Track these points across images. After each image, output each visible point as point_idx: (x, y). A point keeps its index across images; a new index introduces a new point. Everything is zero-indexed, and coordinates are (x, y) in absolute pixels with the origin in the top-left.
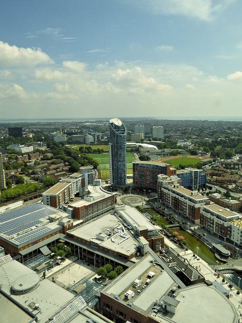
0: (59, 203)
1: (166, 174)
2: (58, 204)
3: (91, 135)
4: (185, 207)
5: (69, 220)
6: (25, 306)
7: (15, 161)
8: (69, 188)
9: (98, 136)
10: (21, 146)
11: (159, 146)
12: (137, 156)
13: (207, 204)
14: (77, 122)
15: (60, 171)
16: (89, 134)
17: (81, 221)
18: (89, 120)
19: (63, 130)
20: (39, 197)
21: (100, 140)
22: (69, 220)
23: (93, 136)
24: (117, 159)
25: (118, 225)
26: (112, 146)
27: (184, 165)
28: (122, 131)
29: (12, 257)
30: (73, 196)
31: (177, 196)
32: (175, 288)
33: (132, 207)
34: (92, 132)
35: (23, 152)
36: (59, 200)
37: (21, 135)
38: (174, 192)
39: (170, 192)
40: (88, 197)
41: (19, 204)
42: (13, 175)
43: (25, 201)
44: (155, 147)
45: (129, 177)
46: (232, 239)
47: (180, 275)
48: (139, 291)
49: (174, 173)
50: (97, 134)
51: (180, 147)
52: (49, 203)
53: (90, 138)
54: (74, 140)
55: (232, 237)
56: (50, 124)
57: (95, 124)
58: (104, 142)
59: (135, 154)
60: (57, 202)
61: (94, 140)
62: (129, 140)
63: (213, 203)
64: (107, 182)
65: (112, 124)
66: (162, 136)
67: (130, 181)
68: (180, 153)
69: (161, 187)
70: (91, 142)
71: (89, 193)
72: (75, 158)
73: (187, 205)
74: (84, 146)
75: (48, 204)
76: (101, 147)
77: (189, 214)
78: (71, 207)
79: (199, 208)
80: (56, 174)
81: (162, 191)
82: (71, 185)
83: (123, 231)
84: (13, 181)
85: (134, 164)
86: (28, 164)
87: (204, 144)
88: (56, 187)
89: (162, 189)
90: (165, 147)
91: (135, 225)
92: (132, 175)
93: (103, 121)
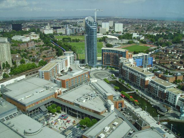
1: (125, 57)
9: (75, 29)
17: (66, 89)
23: (72, 29)
27: (137, 51)
30: (59, 72)
32: (131, 132)
33: (101, 80)
41: (24, 77)
42: (18, 58)
43: (27, 75)
44: (117, 38)
46: (168, 101)
49: (130, 56)
50: (75, 28)
55: (168, 100)
56: (41, 21)
62: (98, 33)
63: (157, 77)
76: (77, 38)
85: (103, 50)
88: (48, 66)
92: (101, 58)
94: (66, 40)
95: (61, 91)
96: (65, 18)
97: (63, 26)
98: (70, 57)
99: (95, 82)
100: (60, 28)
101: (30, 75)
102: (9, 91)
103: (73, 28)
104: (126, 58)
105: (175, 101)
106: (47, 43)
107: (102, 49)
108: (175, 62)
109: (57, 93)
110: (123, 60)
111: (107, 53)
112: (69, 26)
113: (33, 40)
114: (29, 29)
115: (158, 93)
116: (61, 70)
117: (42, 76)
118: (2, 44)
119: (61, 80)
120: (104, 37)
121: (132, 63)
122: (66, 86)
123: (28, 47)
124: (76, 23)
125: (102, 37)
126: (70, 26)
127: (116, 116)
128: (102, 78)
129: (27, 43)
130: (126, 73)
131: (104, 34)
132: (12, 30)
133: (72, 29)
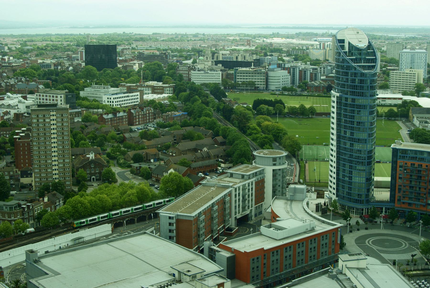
3: (284, 69)
5: (221, 281)
8: (222, 202)
12: (404, 132)
15: (203, 159)
16: (279, 66)
18: (282, 32)
20: (150, 218)
21: (306, 84)
22: (221, 281)
23: (291, 71)
24: (352, 134)
28: (368, 61)
30: (232, 223)
33: (384, 261)
37: (113, 64)
40: (270, 226)
42: (92, 161)
45: (380, 186)
50: (300, 65)
52: (174, 234)
54: (240, 80)
57: (295, 41)
58: (317, 88)
59: (400, 123)
61: (293, 82)
62: (385, 87)
65: (342, 41)
70: (285, 89)
71: (274, 217)
75: (171, 238)
80: (194, 165)
82: (230, 194)
84: (91, 174)
85: (395, 151)
86: (127, 135)
88: (193, 198)
92: (389, 179)
93: (316, 35)
94: (264, 107)
96: (269, 32)
97: (258, 57)
98: (274, 170)
99: (358, 269)
100: (247, 64)
101: (127, 223)
102: (50, 274)
103: (294, 68)
107: (393, 146)
111: (413, 165)
112: (279, 59)
113: (152, 103)
114: (140, 65)
116: (239, 216)
117: (170, 231)
118: (45, 113)
119: (236, 252)
120: (405, 103)
124: (308, 49)
125: (400, 102)
126: (283, 61)
128: (386, 256)
131: (404, 94)
132: (83, 64)
133: (291, 71)
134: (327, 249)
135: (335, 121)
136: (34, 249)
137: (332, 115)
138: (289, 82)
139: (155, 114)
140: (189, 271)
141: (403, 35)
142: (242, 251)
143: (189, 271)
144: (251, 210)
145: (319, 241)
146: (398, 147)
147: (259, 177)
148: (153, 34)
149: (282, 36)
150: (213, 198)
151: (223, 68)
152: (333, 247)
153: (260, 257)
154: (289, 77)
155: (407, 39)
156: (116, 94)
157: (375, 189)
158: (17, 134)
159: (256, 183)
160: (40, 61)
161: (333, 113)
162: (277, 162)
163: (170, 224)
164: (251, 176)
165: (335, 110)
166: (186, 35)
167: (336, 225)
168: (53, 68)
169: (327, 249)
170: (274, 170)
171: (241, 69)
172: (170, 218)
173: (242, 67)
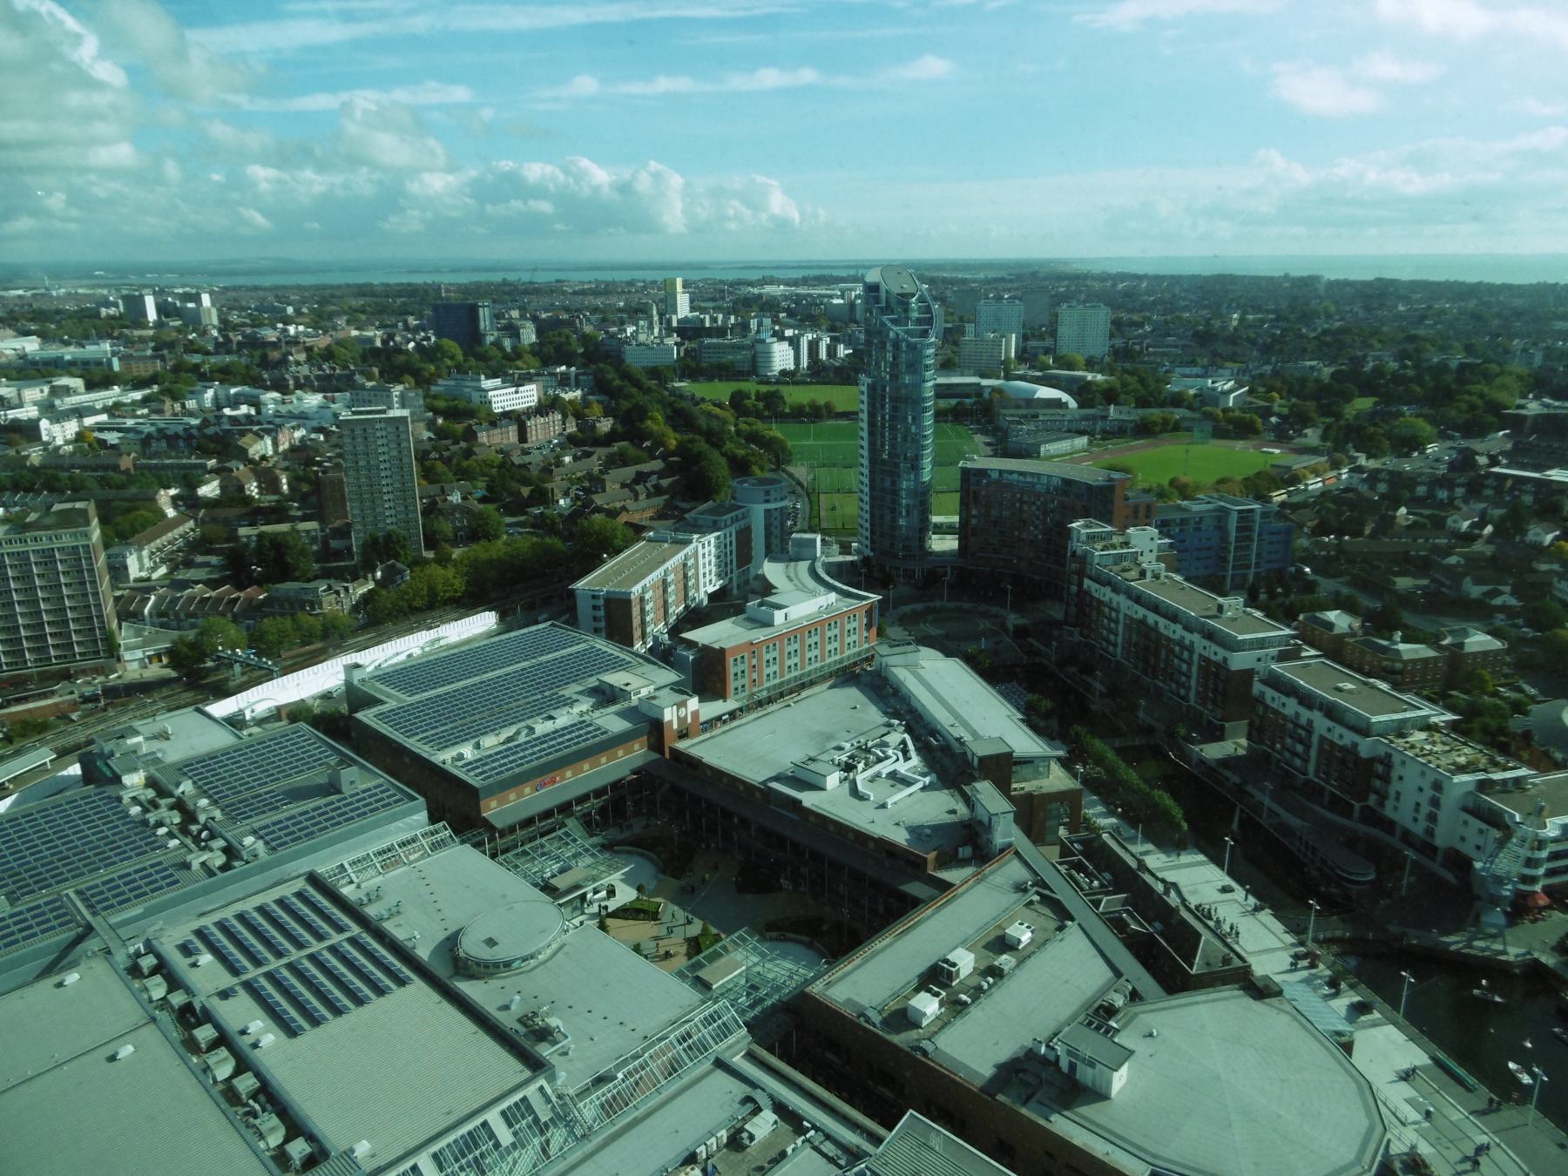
0: (643, 624)
1: (1107, 517)
2: (637, 633)
3: (782, 338)
4: (1184, 667)
6: (508, 1021)
7: (463, 444)
10: (487, 384)
11: (1081, 391)
13: (1282, 657)
14: (722, 282)
16: (775, 334)
17: (731, 704)
19: (661, 315)
23: (794, 343)
25: (885, 730)
26: (872, 388)
29: (457, 831)
31: (1152, 618)
32: (1119, 1001)
34: (790, 327)
35: (497, 408)
36: (642, 610)
38: (1138, 599)
39: (1196, 638)
40: (761, 605)
41: (484, 622)
44: (1065, 397)
46: (1388, 811)
47: (1142, 949)
48: (964, 997)
51: (1177, 400)
52: (602, 624)
53: (782, 357)
55: (1389, 804)
56: (607, 289)
57: (802, 290)
60: (636, 621)
63: (1313, 652)
64: (845, 549)
66: (1099, 345)
67: (943, 544)
68: (1176, 427)
69: (1081, 574)
70: (784, 373)
72: (714, 438)
73: (1195, 658)
74: (750, 387)
77: (1202, 697)
78: (691, 644)
79: (1248, 674)
81: (1084, 594)
83: (905, 752)
85: (965, 471)
87: (1295, 387)
89: (1087, 583)
90: (1110, 396)
91: (958, 732)
92: (955, 519)
95: (695, 714)
96: (754, 276)
98: (768, 512)
104: (1109, 522)
105: (1432, 818)
106: (631, 426)
108: (1453, 560)
109: (675, 726)
110: (1092, 538)
115: (1313, 753)
121: (1149, 562)
122: (732, 684)
123: (526, 446)
127: (1021, 888)
129: (518, 419)
130: (1110, 620)
134: (855, 637)
135: (865, 425)
136: (360, 662)
137: (861, 415)
138: (792, 361)
139: (564, 423)
140: (627, 684)
141: (982, 276)
142: (716, 646)
143: (627, 684)
144: (731, 579)
145: (843, 625)
146: (969, 465)
147: (742, 523)
148: (557, 281)
149: (779, 282)
150: (664, 561)
151: (679, 340)
152: (865, 634)
153: (746, 655)
154: (792, 352)
155: (988, 281)
156: (495, 389)
157: (934, 537)
158: (319, 464)
159: (738, 533)
160: (355, 333)
161: (862, 411)
162: (773, 495)
163: (595, 608)
164: (729, 522)
165: (865, 407)
166: (613, 282)
167: (868, 598)
168: (378, 344)
169: (855, 637)
170: (768, 512)
171: (707, 341)
172: (594, 597)
173: (711, 337)
